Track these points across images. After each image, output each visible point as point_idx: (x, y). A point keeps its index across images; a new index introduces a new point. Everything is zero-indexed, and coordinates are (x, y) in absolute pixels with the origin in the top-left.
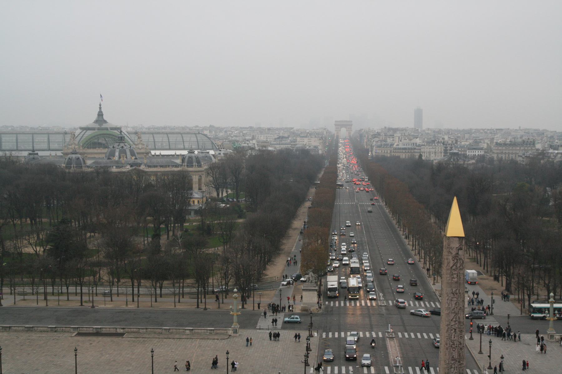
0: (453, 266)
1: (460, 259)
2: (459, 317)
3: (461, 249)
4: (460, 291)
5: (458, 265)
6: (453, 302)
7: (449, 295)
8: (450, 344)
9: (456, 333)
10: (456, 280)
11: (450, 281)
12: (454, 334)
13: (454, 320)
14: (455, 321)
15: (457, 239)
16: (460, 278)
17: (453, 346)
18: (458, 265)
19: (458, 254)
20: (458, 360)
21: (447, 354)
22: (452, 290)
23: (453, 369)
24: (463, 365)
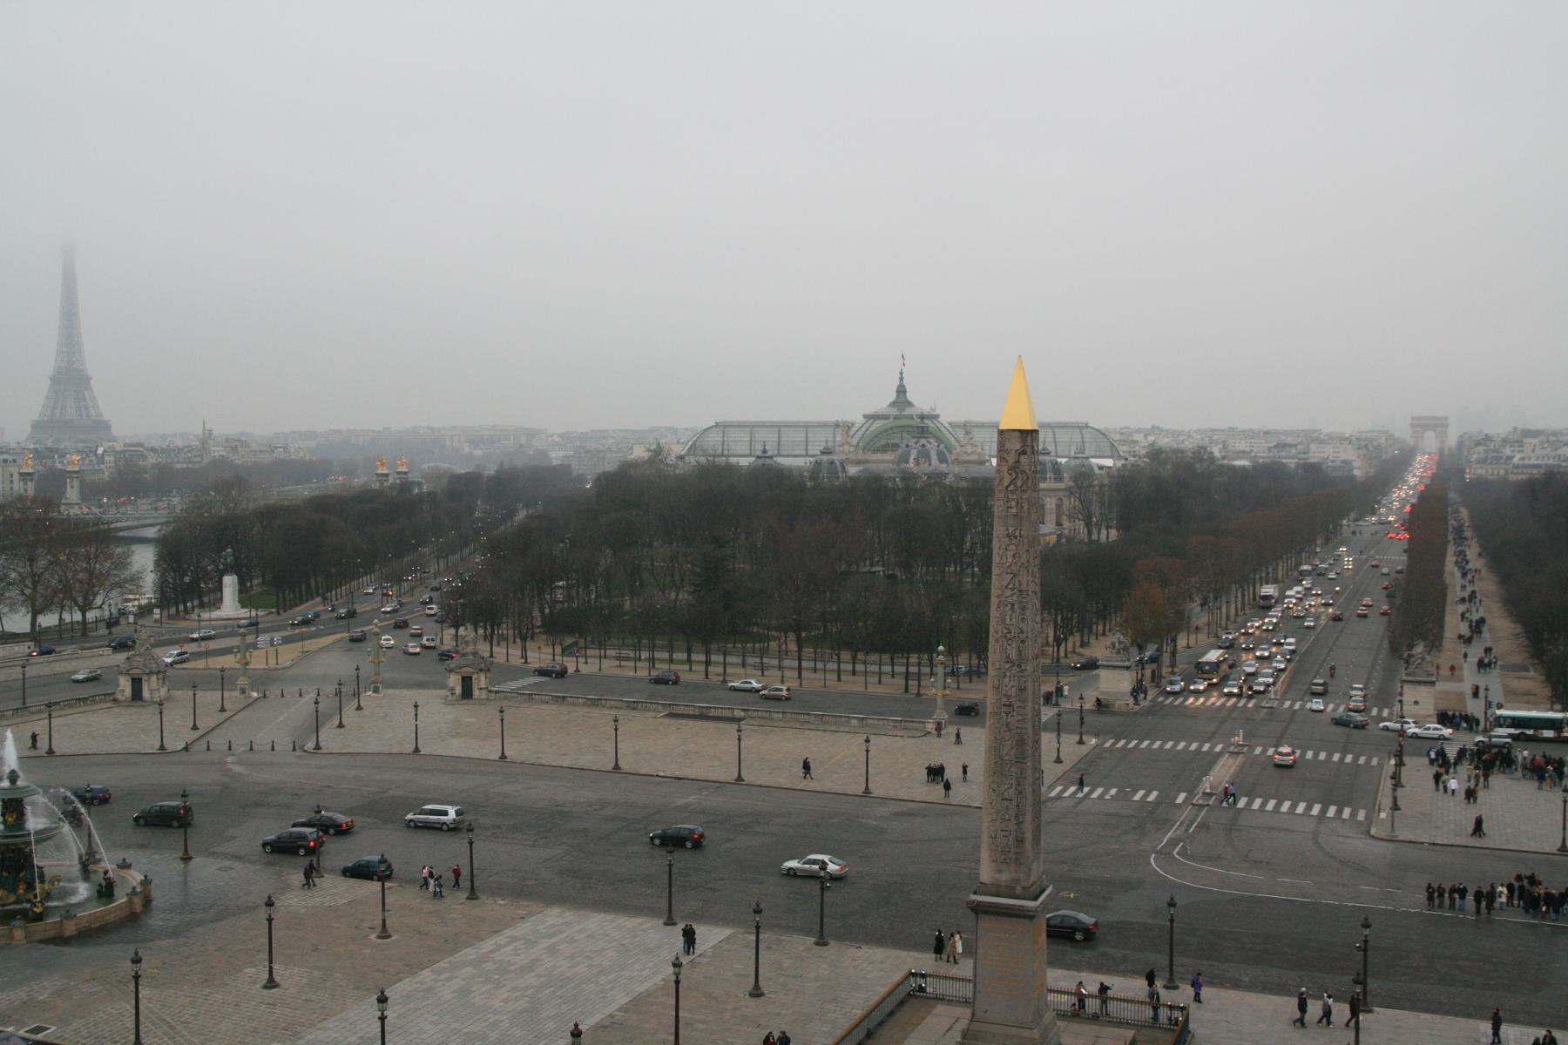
0: (1009, 486)
1: (1023, 472)
2: (1019, 581)
3: (1024, 453)
4: (1022, 533)
5: (1019, 484)
6: (1009, 552)
7: (1003, 540)
8: (1002, 632)
9: (1013, 612)
10: (1014, 510)
11: (1004, 514)
12: (1010, 613)
13: (1011, 586)
14: (1013, 589)
15: (1018, 434)
16: (1022, 507)
17: (1008, 636)
18: (1019, 484)
19: (1018, 462)
20: (1017, 663)
21: (998, 651)
22: (1007, 530)
23: (1007, 680)
24: (1026, 673)
